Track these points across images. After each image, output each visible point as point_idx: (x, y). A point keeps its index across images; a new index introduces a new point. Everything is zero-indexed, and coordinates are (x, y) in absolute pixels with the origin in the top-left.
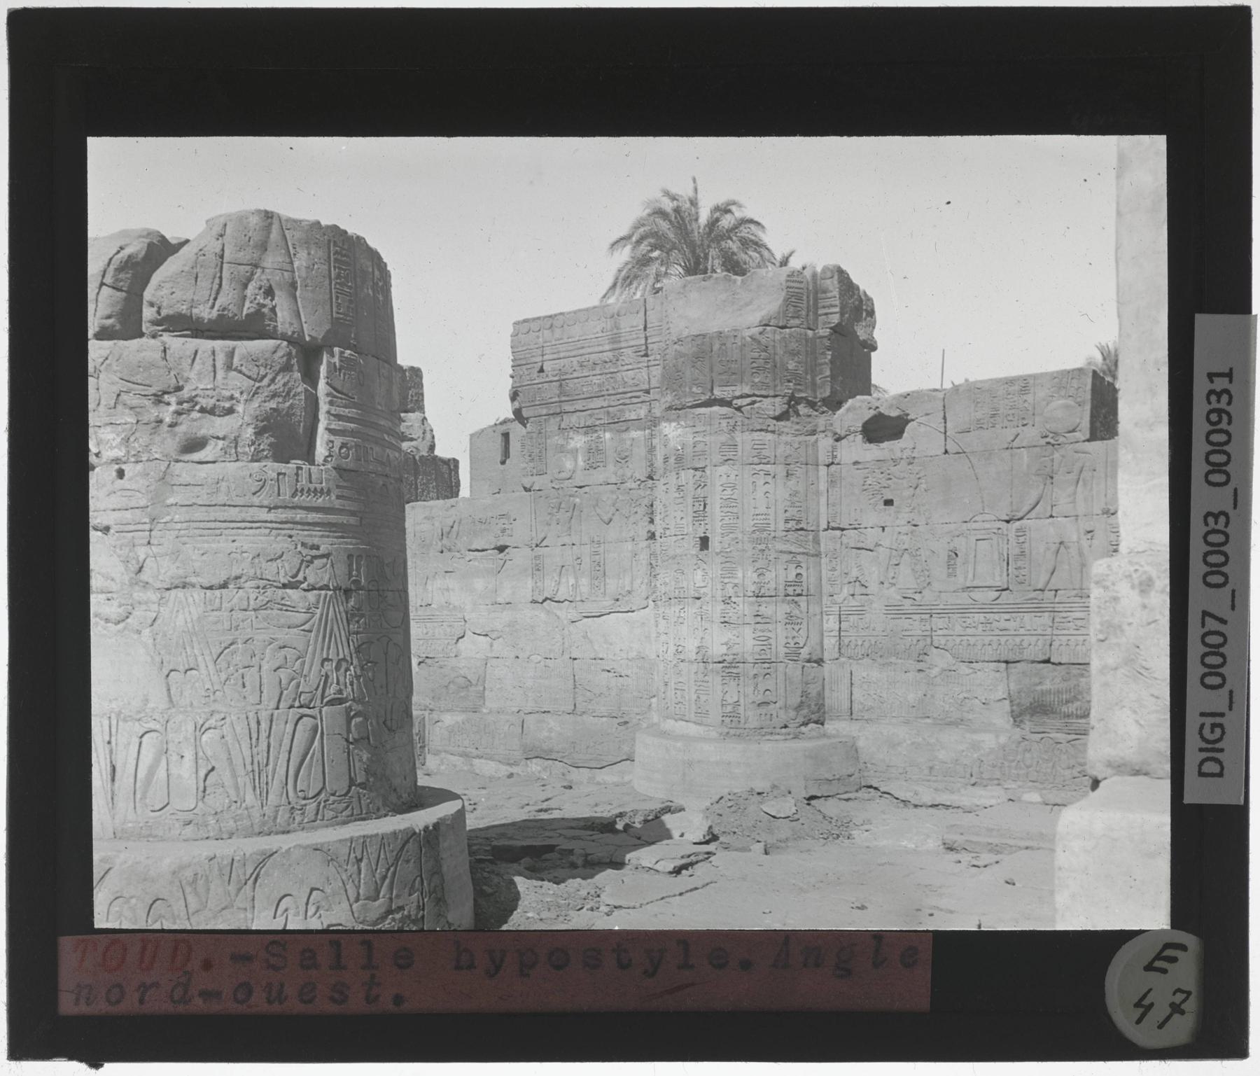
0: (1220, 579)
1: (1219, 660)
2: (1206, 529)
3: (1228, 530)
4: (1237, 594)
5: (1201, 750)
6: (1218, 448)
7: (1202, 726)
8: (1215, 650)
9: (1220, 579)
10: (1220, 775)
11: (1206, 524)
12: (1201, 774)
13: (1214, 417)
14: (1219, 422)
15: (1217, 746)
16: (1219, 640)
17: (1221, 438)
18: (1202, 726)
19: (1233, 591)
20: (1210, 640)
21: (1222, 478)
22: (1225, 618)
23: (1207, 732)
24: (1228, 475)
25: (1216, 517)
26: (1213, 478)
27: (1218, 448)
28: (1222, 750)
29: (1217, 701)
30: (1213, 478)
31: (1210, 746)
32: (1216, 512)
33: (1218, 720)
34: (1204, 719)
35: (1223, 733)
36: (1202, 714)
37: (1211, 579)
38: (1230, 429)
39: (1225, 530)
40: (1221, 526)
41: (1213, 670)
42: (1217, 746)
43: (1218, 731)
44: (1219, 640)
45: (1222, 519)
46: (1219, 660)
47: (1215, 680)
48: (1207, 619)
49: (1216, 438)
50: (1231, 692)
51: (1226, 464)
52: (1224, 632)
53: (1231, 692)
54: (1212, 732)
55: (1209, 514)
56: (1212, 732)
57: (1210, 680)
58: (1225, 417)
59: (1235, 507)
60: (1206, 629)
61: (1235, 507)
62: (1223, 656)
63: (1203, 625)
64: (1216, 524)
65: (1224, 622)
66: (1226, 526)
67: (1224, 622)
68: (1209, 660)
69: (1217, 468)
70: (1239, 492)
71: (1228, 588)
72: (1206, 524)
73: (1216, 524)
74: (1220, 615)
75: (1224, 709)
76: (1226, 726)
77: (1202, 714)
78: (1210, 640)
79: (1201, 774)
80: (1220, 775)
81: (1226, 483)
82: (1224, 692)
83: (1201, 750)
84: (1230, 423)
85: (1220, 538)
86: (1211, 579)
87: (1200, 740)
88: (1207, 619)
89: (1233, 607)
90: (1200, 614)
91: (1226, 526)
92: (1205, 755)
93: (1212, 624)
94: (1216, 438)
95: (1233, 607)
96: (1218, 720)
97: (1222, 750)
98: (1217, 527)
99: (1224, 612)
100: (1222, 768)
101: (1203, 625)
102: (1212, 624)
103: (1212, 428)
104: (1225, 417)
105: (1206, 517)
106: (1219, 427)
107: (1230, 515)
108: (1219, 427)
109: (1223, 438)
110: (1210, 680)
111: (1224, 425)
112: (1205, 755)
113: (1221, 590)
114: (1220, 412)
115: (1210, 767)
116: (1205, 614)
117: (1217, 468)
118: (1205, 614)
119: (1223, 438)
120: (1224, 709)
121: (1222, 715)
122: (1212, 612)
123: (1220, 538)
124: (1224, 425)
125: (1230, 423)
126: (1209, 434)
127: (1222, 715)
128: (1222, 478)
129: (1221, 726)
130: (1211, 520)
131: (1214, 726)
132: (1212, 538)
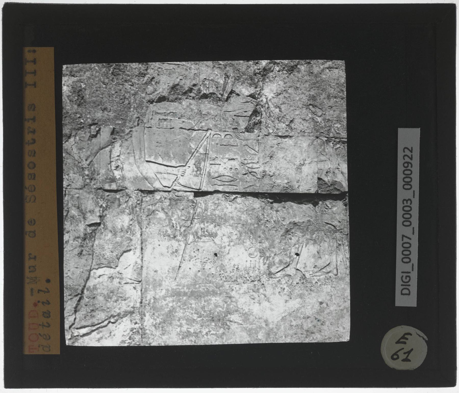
3: (411, 206)
5: (402, 285)
6: (407, 176)
7: (402, 276)
8: (406, 249)
9: (408, 223)
10: (409, 294)
11: (403, 204)
12: (402, 294)
13: (406, 165)
14: (408, 166)
17: (409, 172)
18: (402, 276)
20: (405, 245)
21: (409, 187)
25: (407, 201)
27: (407, 176)
28: (409, 285)
29: (408, 268)
32: (407, 199)
33: (409, 274)
35: (410, 280)
36: (402, 272)
37: (405, 223)
39: (409, 205)
40: (409, 204)
43: (408, 278)
45: (409, 202)
47: (407, 260)
48: (404, 238)
49: (406, 172)
50: (413, 264)
54: (406, 279)
55: (404, 200)
56: (406, 279)
57: (405, 260)
58: (410, 165)
59: (414, 197)
60: (403, 242)
61: (414, 197)
62: (409, 251)
63: (403, 240)
64: (407, 203)
65: (410, 239)
66: (411, 204)
67: (410, 239)
68: (405, 253)
69: (408, 183)
70: (415, 192)
72: (403, 204)
73: (407, 203)
74: (408, 236)
75: (410, 270)
76: (411, 278)
77: (402, 272)
78: (405, 245)
79: (402, 294)
80: (409, 294)
83: (402, 285)
84: (411, 167)
85: (408, 209)
86: (405, 223)
87: (402, 282)
88: (404, 238)
89: (413, 233)
90: (402, 236)
91: (411, 204)
93: (406, 240)
94: (406, 172)
96: (409, 274)
97: (409, 285)
98: (407, 205)
99: (410, 235)
100: (410, 292)
101: (403, 240)
102: (406, 240)
103: (405, 169)
104: (410, 165)
106: (408, 168)
109: (409, 172)
110: (405, 260)
111: (409, 168)
114: (408, 163)
115: (405, 291)
116: (403, 236)
117: (408, 183)
118: (403, 236)
119: (409, 172)
120: (410, 270)
121: (410, 273)
122: (406, 235)
124: (409, 168)
125: (411, 167)
126: (404, 171)
127: (410, 273)
128: (409, 187)
129: (409, 277)
130: (405, 202)
131: (406, 277)
132: (406, 209)
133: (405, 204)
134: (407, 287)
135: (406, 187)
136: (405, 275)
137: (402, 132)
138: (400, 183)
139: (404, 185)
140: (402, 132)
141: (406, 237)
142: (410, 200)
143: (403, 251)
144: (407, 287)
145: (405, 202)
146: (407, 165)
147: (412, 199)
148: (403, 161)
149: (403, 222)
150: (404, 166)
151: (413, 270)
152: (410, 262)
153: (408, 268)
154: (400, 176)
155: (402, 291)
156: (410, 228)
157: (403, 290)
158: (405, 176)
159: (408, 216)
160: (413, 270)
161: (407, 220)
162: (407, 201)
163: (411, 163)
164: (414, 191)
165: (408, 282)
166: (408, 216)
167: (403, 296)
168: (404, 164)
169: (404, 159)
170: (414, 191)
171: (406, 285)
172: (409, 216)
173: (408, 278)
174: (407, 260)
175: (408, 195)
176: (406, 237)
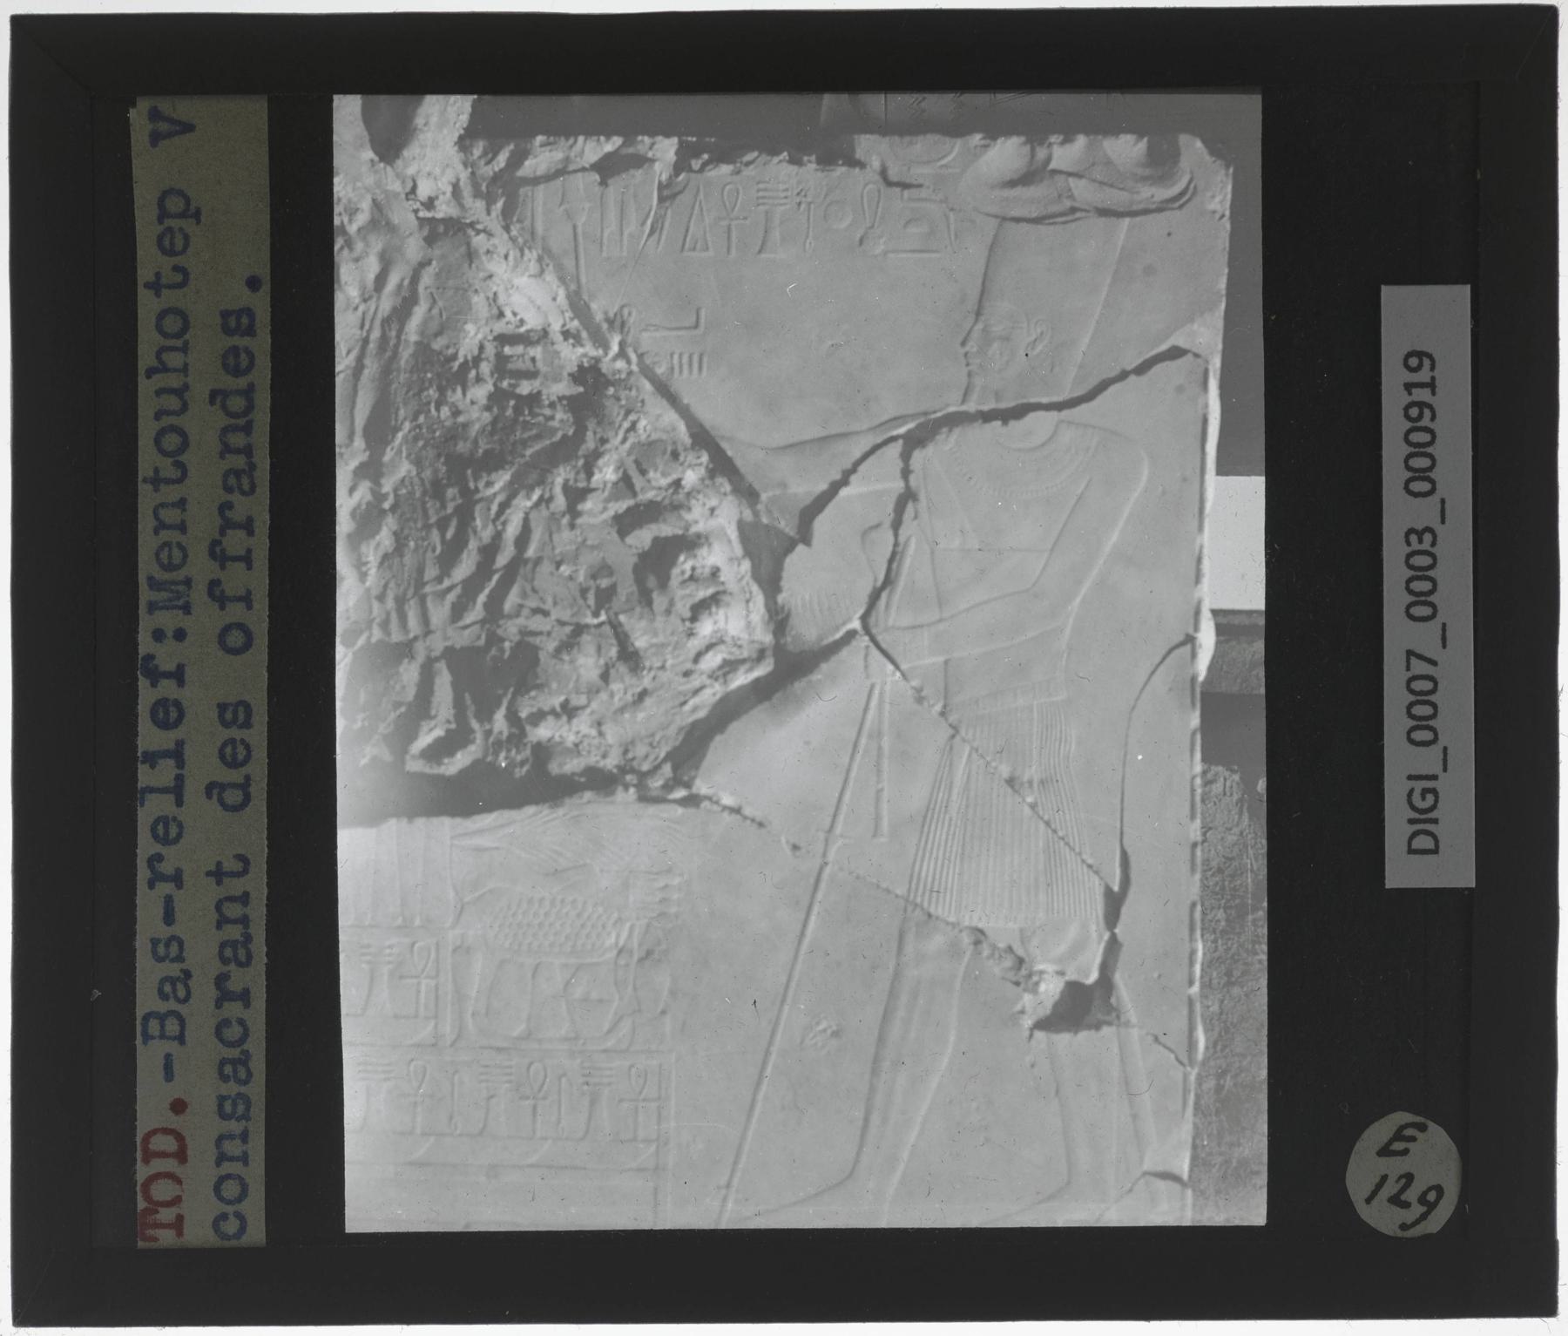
1: (1427, 711)
2: (1408, 550)
3: (1433, 550)
4: (1448, 634)
5: (1411, 821)
6: (1419, 450)
7: (1412, 791)
8: (1422, 698)
10: (1435, 851)
11: (1408, 543)
12: (1411, 851)
13: (1414, 412)
14: (1421, 416)
15: (1430, 815)
16: (1428, 685)
17: (1423, 437)
18: (1412, 791)
19: (1444, 625)
21: (1426, 486)
22: (1435, 658)
24: (1433, 482)
25: (1420, 535)
28: (1435, 821)
29: (1428, 760)
31: (1417, 816)
32: (1420, 527)
34: (1413, 783)
35: (1436, 801)
36: (1410, 778)
40: (1426, 546)
41: (1422, 723)
42: (1430, 815)
43: (1430, 798)
44: (1428, 685)
45: (1427, 537)
46: (1427, 711)
47: (1425, 735)
49: (1415, 437)
50: (1445, 749)
51: (1431, 468)
52: (1431, 673)
53: (1445, 749)
54: (1424, 799)
55: (1411, 531)
56: (1424, 799)
58: (1427, 412)
59: (1443, 522)
60: (1410, 674)
61: (1443, 522)
62: (1434, 706)
63: (1408, 669)
64: (1421, 541)
65: (1434, 663)
66: (1433, 544)
67: (1434, 663)
69: (1422, 475)
71: (1440, 619)
72: (1408, 543)
73: (1421, 541)
74: (1428, 654)
75: (1437, 769)
76: (1440, 795)
77: (1410, 778)
78: (1419, 685)
80: (1435, 851)
82: (1436, 750)
83: (1411, 821)
84: (1433, 418)
85: (1426, 561)
88: (1413, 660)
89: (1444, 646)
91: (1433, 544)
93: (1419, 667)
94: (1415, 437)
95: (1444, 646)
97: (1435, 821)
99: (1431, 648)
101: (1408, 669)
102: (1419, 667)
104: (1427, 412)
106: (1419, 424)
107: (1437, 532)
109: (1426, 437)
111: (1425, 422)
114: (1421, 405)
115: (1423, 842)
116: (1410, 653)
118: (1410, 653)
119: (1423, 437)
120: (1437, 769)
121: (1434, 777)
123: (1426, 561)
124: (1425, 422)
125: (1433, 418)
128: (1426, 486)
129: (1434, 791)
130: (1413, 538)
131: (1425, 792)
133: (1416, 546)
135: (1418, 486)
136: (1420, 785)
137: (1392, 297)
138: (1393, 473)
139: (1408, 482)
140: (1392, 297)
141: (1420, 657)
142: (1429, 530)
143: (1411, 705)
145: (1413, 538)
146: (1418, 413)
148: (1407, 399)
149: (1409, 733)
150: (1407, 417)
151: (1445, 770)
152: (1434, 741)
153: (1428, 760)
154: (1393, 451)
156: (1435, 626)
157: (1415, 835)
158: (1415, 723)
159: (1425, 586)
160: (1445, 770)
161: (1421, 599)
163: (1430, 407)
164: (1443, 501)
165: (1433, 808)
166: (1425, 586)
168: (1407, 408)
170: (1443, 501)
171: (1424, 819)
175: (1423, 513)
176: (1420, 657)
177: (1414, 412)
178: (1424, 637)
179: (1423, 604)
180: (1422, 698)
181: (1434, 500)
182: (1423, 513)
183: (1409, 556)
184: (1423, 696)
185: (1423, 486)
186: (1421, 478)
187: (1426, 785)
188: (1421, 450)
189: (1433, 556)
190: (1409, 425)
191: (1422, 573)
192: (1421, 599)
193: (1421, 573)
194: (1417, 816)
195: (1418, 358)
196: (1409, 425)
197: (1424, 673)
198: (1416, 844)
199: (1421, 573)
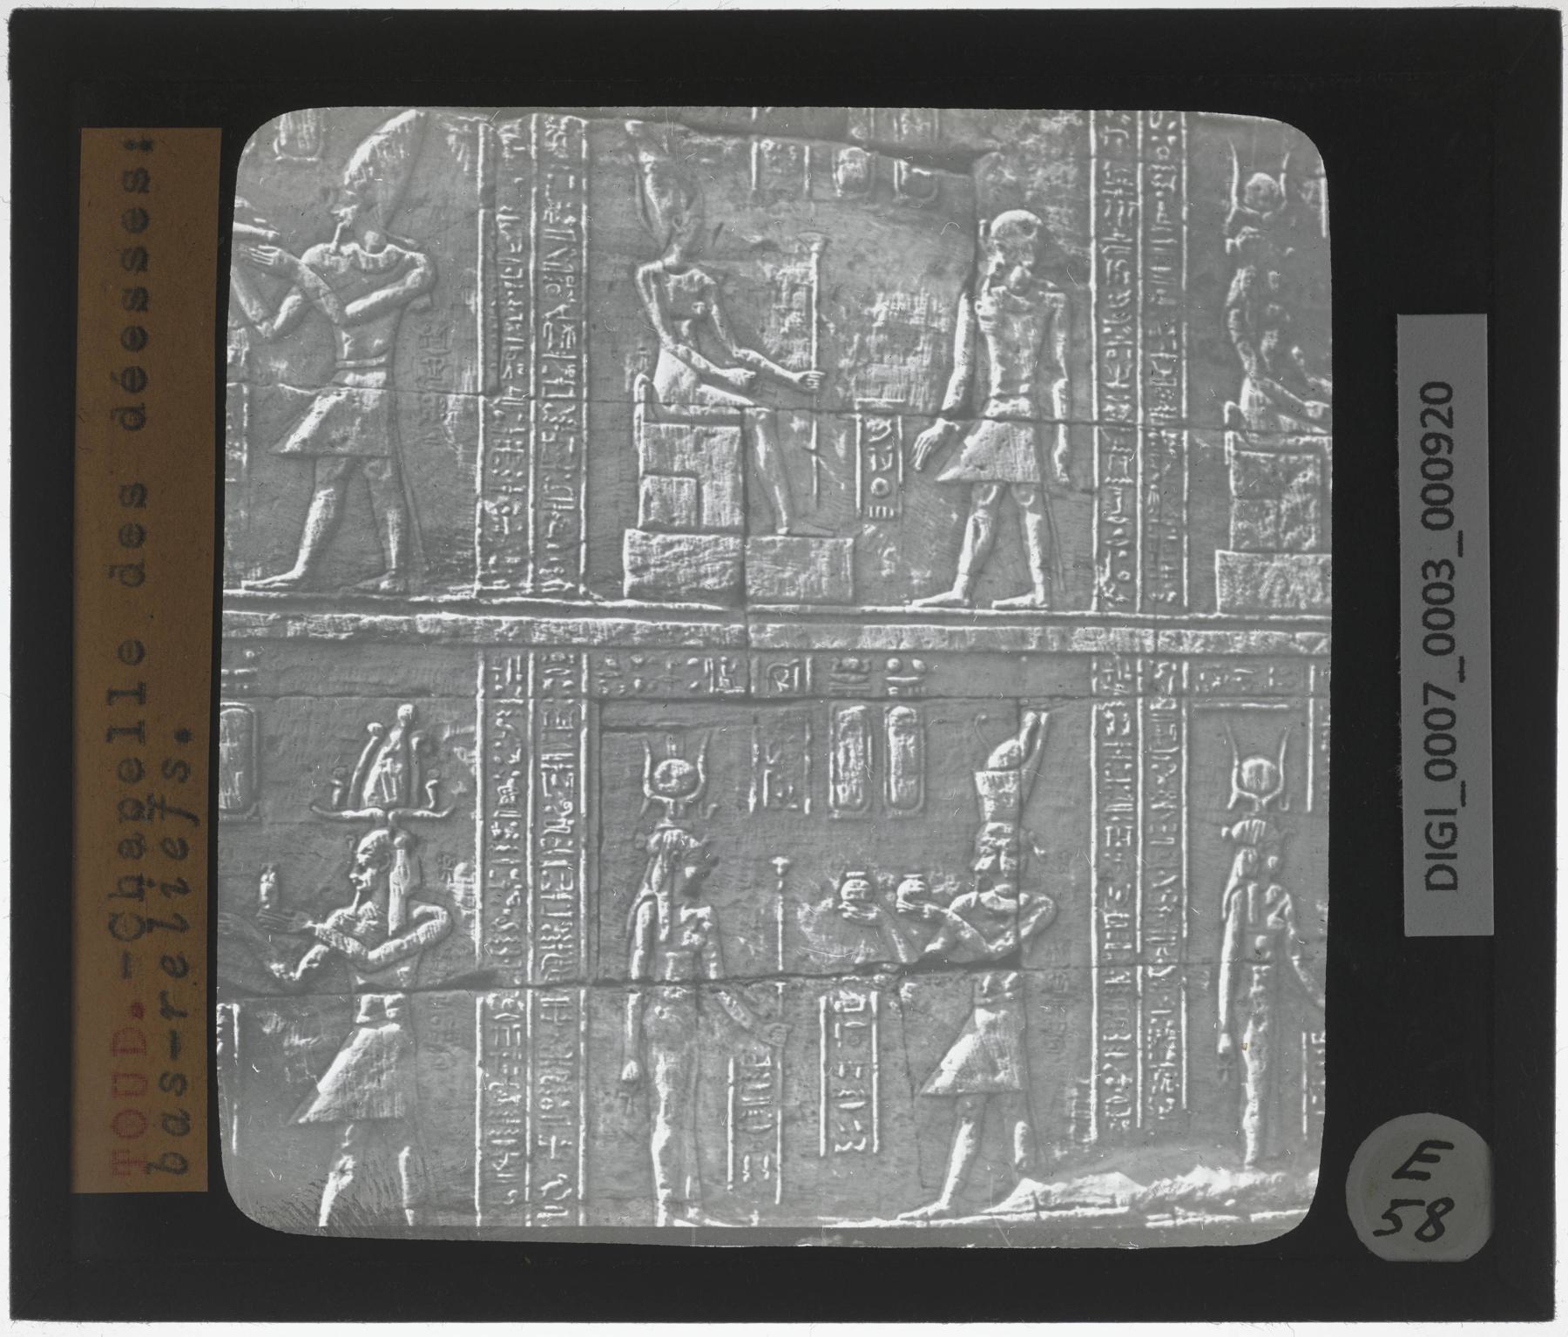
0: (1445, 644)
2: (1426, 583)
3: (1455, 583)
5: (1429, 856)
6: (1437, 482)
7: (1429, 826)
11: (1425, 577)
12: (1430, 887)
13: (1431, 444)
14: (1438, 449)
15: (1446, 851)
16: (1443, 719)
18: (1429, 826)
21: (1443, 519)
23: (1434, 833)
26: (1432, 519)
27: (1437, 482)
28: (1454, 856)
29: (1446, 795)
30: (1432, 519)
31: (1437, 851)
35: (1454, 835)
36: (1428, 812)
38: (1447, 457)
40: (1444, 578)
41: (1440, 757)
42: (1446, 851)
43: (1448, 832)
44: (1443, 719)
45: (1445, 570)
47: (1446, 770)
48: (1431, 694)
50: (1463, 784)
51: (1449, 500)
53: (1463, 784)
54: (1442, 834)
55: (1429, 563)
56: (1442, 834)
58: (1444, 444)
59: (1460, 554)
61: (1460, 554)
62: (1452, 740)
63: (1426, 702)
64: (1438, 575)
65: (1451, 697)
66: (1450, 578)
67: (1451, 697)
72: (1425, 577)
73: (1438, 575)
75: (1457, 805)
77: (1428, 812)
80: (1454, 887)
81: (1449, 524)
82: (1452, 787)
83: (1429, 856)
84: (1450, 451)
85: (1444, 594)
88: (1431, 694)
89: (1462, 679)
90: (1421, 691)
91: (1450, 578)
92: (1433, 862)
93: (1436, 701)
95: (1462, 679)
97: (1454, 856)
99: (1447, 681)
100: (1455, 878)
101: (1426, 702)
102: (1436, 701)
104: (1444, 444)
105: (1424, 569)
106: (1440, 455)
108: (1440, 455)
110: (1438, 770)
111: (1443, 454)
112: (1433, 862)
113: (1448, 656)
115: (1441, 877)
116: (1427, 687)
118: (1427, 687)
121: (1453, 812)
123: (1444, 594)
124: (1443, 454)
125: (1450, 451)
128: (1443, 519)
129: (1452, 826)
130: (1431, 571)
131: (1442, 826)
133: (1433, 579)
134: (1447, 862)
135: (1435, 519)
136: (1437, 820)
141: (1438, 691)
142: (1447, 562)
144: (1447, 862)
147: (1454, 558)
151: (1464, 804)
153: (1446, 795)
155: (1428, 876)
156: (1451, 661)
157: (1431, 872)
160: (1464, 804)
162: (1437, 568)
163: (1448, 439)
164: (1461, 533)
167: (1436, 893)
169: (1424, 425)
170: (1461, 533)
171: (1442, 853)
172: (1445, 619)
173: (1448, 832)
174: (1446, 770)
175: (1441, 545)
176: (1438, 691)
177: (1431, 444)
178: (1442, 671)
179: (1440, 637)
180: (1438, 732)
181: (1450, 535)
182: (1441, 545)
183: (1426, 589)
184: (1440, 730)
185: (1441, 519)
186: (1438, 510)
187: (1445, 821)
188: (1438, 480)
189: (1450, 588)
190: (1425, 457)
191: (1439, 606)
192: (1439, 632)
193: (1438, 606)
194: (1437, 851)
195: (1437, 396)
196: (1425, 457)
197: (1438, 706)
198: (1438, 878)
199: (1438, 606)
